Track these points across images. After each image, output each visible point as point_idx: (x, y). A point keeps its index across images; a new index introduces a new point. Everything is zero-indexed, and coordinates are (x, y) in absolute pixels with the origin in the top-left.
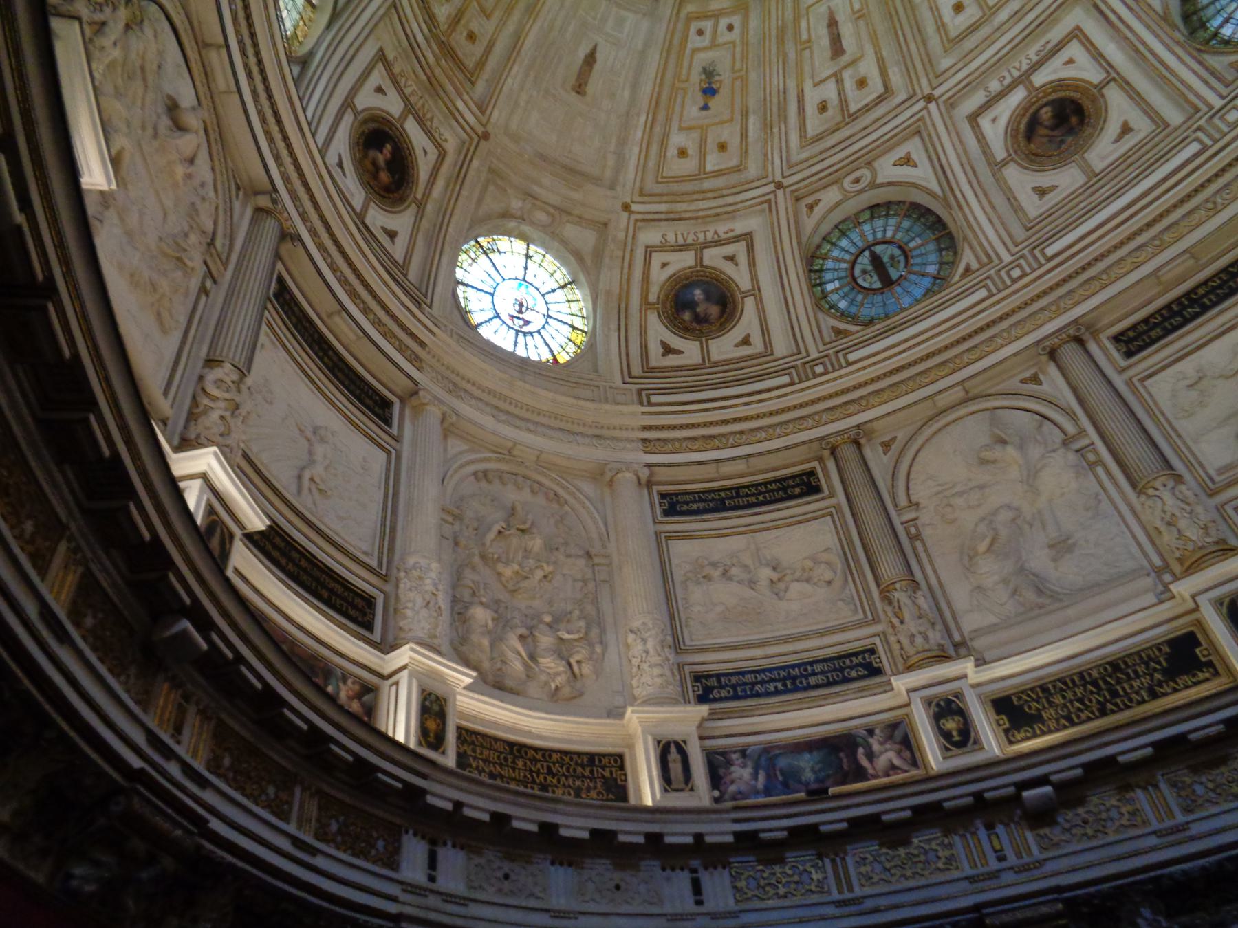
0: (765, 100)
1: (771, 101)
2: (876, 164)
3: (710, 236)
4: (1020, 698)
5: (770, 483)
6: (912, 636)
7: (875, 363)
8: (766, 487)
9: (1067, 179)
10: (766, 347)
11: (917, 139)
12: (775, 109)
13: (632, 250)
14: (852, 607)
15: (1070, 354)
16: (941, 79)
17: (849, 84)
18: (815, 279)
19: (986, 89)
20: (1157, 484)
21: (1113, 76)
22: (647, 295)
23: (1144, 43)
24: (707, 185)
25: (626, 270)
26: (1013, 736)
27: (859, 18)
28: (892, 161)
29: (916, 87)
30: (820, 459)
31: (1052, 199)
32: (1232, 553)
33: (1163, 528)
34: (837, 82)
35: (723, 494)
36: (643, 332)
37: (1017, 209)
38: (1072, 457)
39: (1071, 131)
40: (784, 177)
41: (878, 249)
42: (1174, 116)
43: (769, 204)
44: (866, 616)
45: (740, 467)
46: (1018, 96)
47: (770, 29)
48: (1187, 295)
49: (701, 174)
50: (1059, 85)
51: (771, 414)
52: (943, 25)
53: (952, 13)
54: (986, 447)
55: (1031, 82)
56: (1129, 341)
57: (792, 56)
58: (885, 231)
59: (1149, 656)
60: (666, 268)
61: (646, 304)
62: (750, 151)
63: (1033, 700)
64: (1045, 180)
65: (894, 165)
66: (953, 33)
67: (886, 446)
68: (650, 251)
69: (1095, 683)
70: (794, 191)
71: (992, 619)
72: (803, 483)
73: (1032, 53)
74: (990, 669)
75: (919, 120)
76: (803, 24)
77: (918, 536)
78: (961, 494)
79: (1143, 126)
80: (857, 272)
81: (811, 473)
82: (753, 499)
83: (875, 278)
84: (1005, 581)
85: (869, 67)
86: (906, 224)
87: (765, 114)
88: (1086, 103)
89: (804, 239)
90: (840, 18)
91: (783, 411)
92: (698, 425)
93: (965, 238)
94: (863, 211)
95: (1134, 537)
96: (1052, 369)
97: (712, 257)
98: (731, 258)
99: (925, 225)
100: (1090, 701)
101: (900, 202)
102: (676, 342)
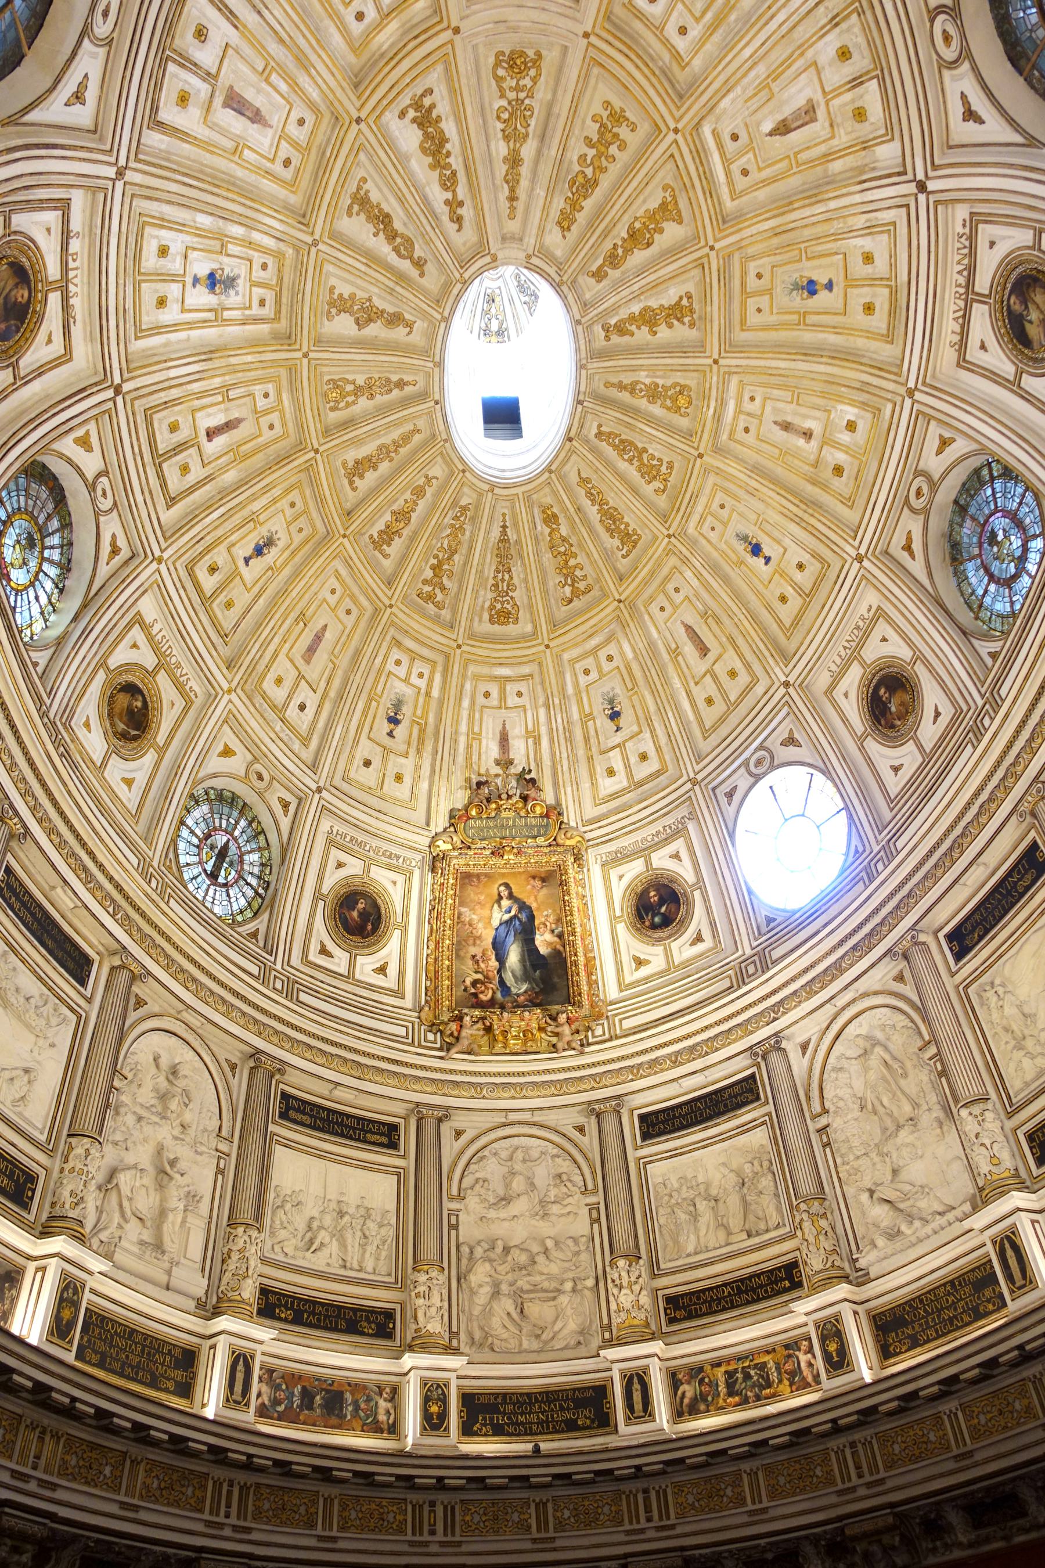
34: (209, 74)
46: (53, 271)
47: (319, 56)
55: (56, 289)
57: (274, 48)
66: (148, 230)
75: (111, 150)
76: (283, 87)
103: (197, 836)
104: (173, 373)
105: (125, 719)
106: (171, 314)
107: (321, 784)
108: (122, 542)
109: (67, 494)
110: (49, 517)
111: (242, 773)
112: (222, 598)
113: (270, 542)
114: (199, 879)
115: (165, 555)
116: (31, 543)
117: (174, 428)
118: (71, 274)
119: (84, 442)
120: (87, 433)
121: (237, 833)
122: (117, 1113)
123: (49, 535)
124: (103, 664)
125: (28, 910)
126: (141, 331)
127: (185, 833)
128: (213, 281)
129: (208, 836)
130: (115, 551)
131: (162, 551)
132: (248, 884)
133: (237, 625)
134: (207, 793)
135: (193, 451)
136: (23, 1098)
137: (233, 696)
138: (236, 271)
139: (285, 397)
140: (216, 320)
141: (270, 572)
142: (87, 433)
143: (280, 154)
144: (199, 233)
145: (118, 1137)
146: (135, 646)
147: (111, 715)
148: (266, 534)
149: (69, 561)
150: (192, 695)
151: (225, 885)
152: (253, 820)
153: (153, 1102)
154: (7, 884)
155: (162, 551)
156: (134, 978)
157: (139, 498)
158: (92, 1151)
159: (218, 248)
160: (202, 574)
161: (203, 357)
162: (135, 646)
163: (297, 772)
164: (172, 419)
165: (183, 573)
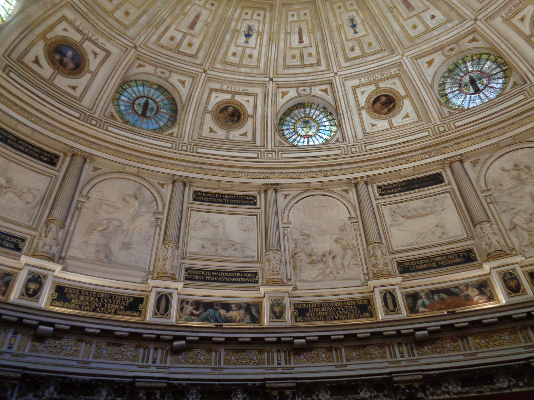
0: (156, 15)
1: (157, 18)
2: (173, 74)
3: (94, 38)
4: (68, 290)
5: (36, 147)
6: (46, 244)
7: (116, 138)
8: (33, 148)
9: (221, 133)
10: (80, 96)
11: (191, 79)
12: (156, 22)
13: (56, 11)
14: (30, 218)
15: (179, 185)
16: (213, 69)
17: (186, 41)
18: (120, 91)
19: (222, 86)
20: (171, 245)
21: (254, 117)
22: (46, 34)
23: (267, 116)
24: (110, 20)
25: (46, 15)
26: (55, 303)
27: (205, 24)
28: (178, 78)
29: (204, 64)
30: (65, 155)
31: (212, 135)
32: (174, 280)
33: (161, 260)
35: (10, 136)
36: (32, 45)
37: (201, 129)
38: (153, 219)
39: (233, 121)
40: (139, 46)
41: (150, 101)
42: (258, 143)
43: (126, 50)
44: (32, 226)
45: (28, 132)
46: (228, 97)
48: (223, 194)
49: (111, 14)
50: (240, 105)
51: (60, 123)
52: (227, 55)
53: (232, 54)
54: (129, 196)
55: (234, 96)
56: (197, 196)
57: (177, 12)
58: (157, 97)
59: (124, 299)
60: (65, 32)
61: (43, 36)
62: (136, 25)
63: (73, 293)
64: (215, 128)
65: (178, 80)
66: (227, 60)
67: (95, 169)
68: (64, 18)
69: (99, 299)
70: (139, 55)
71: (82, 256)
72: (50, 158)
73: (242, 88)
74: (67, 274)
75: (197, 74)
76: (189, 6)
77: (80, 209)
78: (107, 205)
79: (249, 138)
80: (137, 102)
81: (57, 157)
82: (23, 148)
83: (141, 110)
84: (98, 245)
85: (196, 42)
86: (166, 102)
87: (152, 20)
88: (242, 117)
89: (128, 74)
90: (201, 18)
91: (66, 125)
92: (24, 101)
93: (179, 124)
94: (156, 84)
95: (151, 257)
96: (170, 187)
97: (88, 46)
98: (95, 54)
99: (171, 107)
100: (93, 304)
101: (169, 93)
102: (43, 61)
103: (456, 91)
104: (273, 56)
105: (384, 108)
106: (255, 53)
107: (473, 17)
108: (324, 87)
109: (301, 102)
110: (304, 112)
111: (444, 58)
112: (366, 47)
113: (352, 20)
114: (472, 99)
115: (335, 71)
116: (307, 122)
117: (294, 57)
118: (233, 90)
119: (284, 94)
120: (282, 92)
121: (470, 69)
122: (496, 202)
123: (309, 114)
124: (359, 108)
125: (399, 187)
126: (257, 66)
127: (450, 96)
128: (248, 36)
129: (460, 86)
130: (325, 91)
131: (333, 72)
132: (495, 74)
133: (379, 42)
134: (444, 77)
135: (304, 50)
136: (443, 233)
137: (406, 54)
138: (246, 26)
139: (296, 7)
140: (261, 35)
141: (365, 23)
142: (282, 92)
143: (209, 8)
144: (231, 40)
145: (504, 208)
146: (363, 92)
147: (379, 113)
148: (348, 22)
149: (324, 107)
150: (397, 72)
151: (486, 86)
152: (472, 57)
153: (515, 183)
154: (383, 190)
155: (333, 72)
156: (461, 162)
157: (310, 78)
158: (483, 226)
159: (238, 33)
160: (352, 55)
161: (271, 43)
162: (363, 92)
163: (459, 30)
164: (291, 57)
165: (348, 64)
